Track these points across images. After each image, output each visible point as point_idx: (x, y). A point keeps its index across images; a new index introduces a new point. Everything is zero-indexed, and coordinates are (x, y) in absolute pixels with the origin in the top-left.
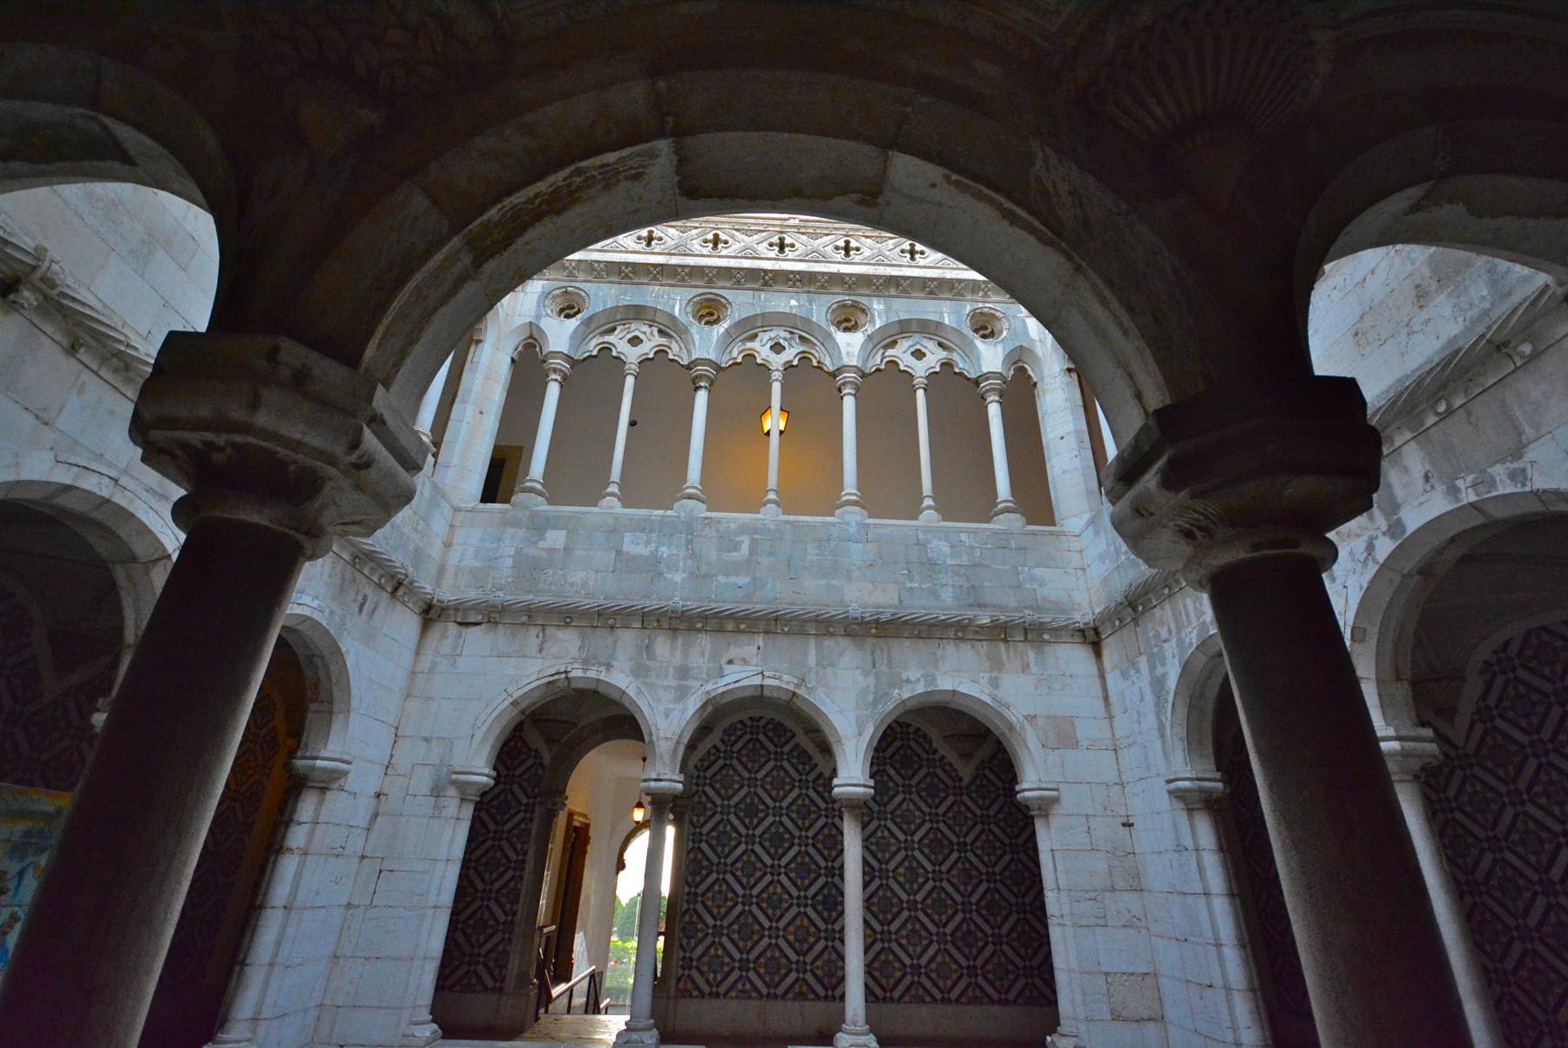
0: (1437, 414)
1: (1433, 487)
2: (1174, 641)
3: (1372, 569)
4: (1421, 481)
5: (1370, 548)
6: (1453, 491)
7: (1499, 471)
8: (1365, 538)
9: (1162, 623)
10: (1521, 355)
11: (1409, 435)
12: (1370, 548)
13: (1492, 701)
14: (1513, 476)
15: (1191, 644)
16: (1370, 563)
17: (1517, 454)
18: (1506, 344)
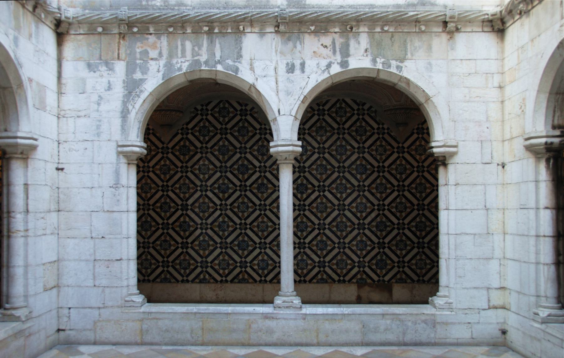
0: (382, 29)
1: (367, 56)
2: (162, 62)
3: (326, 75)
4: (363, 51)
5: (329, 66)
6: (374, 61)
7: (394, 63)
8: (328, 61)
9: (154, 47)
10: (420, 29)
11: (367, 30)
12: (329, 66)
13: (190, 126)
14: (398, 67)
15: (180, 69)
16: (326, 73)
17: (402, 62)
18: (419, 22)
